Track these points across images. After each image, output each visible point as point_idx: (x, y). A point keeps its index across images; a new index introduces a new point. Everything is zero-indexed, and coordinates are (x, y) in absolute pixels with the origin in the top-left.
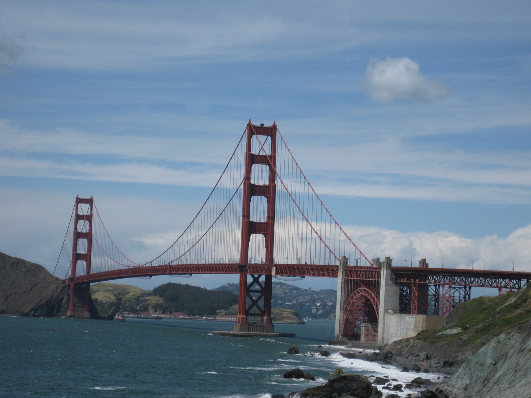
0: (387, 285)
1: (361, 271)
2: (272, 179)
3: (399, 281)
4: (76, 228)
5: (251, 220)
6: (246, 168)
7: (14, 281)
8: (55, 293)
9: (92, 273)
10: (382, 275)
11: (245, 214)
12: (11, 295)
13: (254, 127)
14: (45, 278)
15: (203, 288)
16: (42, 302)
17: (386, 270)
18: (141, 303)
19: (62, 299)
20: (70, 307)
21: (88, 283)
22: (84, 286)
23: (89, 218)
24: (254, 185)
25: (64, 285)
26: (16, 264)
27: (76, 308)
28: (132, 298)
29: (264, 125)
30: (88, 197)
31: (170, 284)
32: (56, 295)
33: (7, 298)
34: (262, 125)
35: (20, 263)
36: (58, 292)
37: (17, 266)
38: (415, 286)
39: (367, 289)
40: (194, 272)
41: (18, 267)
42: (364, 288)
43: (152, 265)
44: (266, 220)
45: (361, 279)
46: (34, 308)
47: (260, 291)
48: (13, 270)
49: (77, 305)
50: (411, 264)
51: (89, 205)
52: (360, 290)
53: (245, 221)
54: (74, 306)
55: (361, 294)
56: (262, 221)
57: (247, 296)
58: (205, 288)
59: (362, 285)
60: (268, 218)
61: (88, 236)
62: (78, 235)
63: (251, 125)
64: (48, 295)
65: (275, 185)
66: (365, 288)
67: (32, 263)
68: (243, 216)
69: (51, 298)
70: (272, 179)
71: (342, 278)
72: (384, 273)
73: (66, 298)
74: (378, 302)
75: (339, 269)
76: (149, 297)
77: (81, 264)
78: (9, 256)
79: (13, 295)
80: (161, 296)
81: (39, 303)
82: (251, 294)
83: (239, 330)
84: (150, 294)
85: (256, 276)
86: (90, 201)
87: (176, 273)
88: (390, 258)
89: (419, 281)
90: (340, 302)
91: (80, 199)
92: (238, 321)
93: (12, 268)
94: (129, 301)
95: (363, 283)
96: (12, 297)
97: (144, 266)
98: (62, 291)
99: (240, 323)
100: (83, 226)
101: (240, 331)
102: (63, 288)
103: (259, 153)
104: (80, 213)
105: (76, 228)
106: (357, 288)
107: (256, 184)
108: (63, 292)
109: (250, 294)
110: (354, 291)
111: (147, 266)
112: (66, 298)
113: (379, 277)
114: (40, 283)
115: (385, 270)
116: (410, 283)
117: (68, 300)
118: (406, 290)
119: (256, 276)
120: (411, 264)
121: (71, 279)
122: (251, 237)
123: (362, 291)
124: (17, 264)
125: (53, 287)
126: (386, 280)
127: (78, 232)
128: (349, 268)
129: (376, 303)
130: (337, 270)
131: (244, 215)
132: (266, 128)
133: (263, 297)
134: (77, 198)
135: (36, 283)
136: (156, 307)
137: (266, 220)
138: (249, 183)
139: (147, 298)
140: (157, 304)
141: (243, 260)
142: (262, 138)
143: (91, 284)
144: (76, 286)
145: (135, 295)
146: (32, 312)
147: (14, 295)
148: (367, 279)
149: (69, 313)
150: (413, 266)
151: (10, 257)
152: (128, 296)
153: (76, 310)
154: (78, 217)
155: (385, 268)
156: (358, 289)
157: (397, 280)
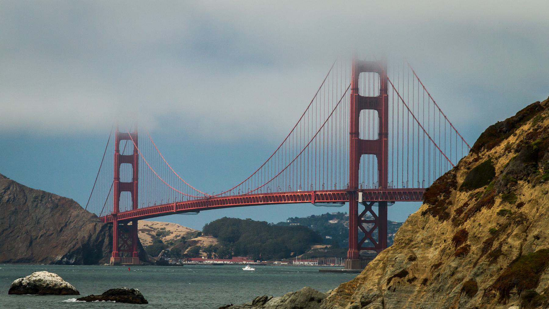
2: (384, 90)
5: (362, 137)
6: (353, 78)
7: (38, 221)
8: (93, 234)
9: (139, 207)
11: (354, 131)
12: (36, 238)
14: (78, 216)
16: (77, 247)
18: (190, 246)
19: (103, 241)
20: (114, 252)
21: (135, 221)
22: (130, 224)
25: (104, 224)
26: (40, 198)
27: (121, 253)
28: (175, 239)
31: (225, 219)
32: (94, 237)
33: (31, 242)
35: (44, 197)
36: (97, 232)
37: (41, 200)
40: (289, 202)
41: (43, 202)
44: (376, 137)
46: (67, 254)
48: (37, 206)
49: (122, 248)
53: (353, 139)
54: (119, 249)
57: (358, 227)
58: (273, 223)
60: (380, 134)
61: (133, 160)
62: (121, 159)
64: (84, 236)
65: (388, 95)
68: (351, 133)
69: (88, 240)
70: (384, 90)
73: (107, 241)
76: (199, 238)
77: (126, 196)
78: (30, 188)
79: (39, 237)
80: (215, 236)
81: (73, 248)
83: (351, 267)
84: (199, 234)
87: (264, 203)
92: (349, 257)
93: (35, 203)
94: (172, 244)
96: (38, 240)
97: (220, 196)
98: (101, 231)
101: (352, 268)
102: (103, 227)
105: (117, 150)
108: (103, 233)
111: (223, 195)
112: (107, 241)
114: (73, 222)
117: (111, 243)
119: (368, 203)
121: (115, 215)
122: (362, 158)
124: (42, 198)
125: (90, 226)
127: (120, 155)
131: (353, 133)
133: (378, 227)
135: (67, 222)
136: (210, 250)
137: (376, 137)
138: (357, 95)
139: (196, 239)
140: (211, 246)
141: (353, 185)
143: (139, 222)
144: (120, 224)
145: (179, 236)
146: (66, 259)
147: (39, 238)
149: (112, 259)
151: (31, 190)
152: (168, 238)
153: (121, 255)
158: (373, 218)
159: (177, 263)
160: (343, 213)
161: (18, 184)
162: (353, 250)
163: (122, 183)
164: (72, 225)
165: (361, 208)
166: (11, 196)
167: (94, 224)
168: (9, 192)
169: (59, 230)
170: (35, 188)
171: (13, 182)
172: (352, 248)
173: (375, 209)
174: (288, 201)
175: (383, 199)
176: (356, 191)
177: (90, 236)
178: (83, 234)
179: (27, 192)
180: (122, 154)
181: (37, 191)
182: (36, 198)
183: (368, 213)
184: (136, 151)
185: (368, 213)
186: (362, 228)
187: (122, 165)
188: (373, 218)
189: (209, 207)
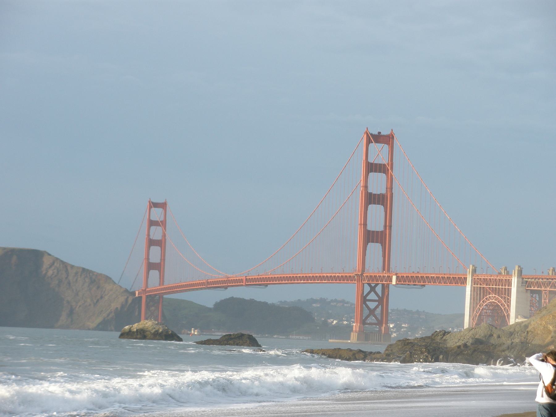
0: (518, 292)
1: (490, 279)
2: (390, 188)
3: (529, 288)
4: (149, 235)
10: (513, 283)
11: (362, 223)
13: (371, 134)
15: (270, 304)
16: (110, 316)
17: (517, 278)
23: (163, 224)
24: (371, 194)
29: (382, 134)
30: (162, 201)
31: (232, 299)
34: (379, 133)
36: (128, 304)
37: (81, 275)
38: (545, 293)
39: (497, 296)
40: (301, 282)
42: (494, 295)
43: (248, 274)
45: (491, 286)
47: (368, 301)
48: (77, 280)
50: (543, 272)
51: (162, 209)
52: (489, 297)
55: (491, 301)
56: (377, 230)
59: (492, 293)
60: (385, 226)
61: (160, 243)
62: (151, 243)
63: (369, 134)
66: (495, 296)
67: (98, 273)
71: (471, 285)
72: (515, 281)
74: (509, 309)
75: (468, 277)
77: (154, 274)
79: (78, 307)
82: (367, 303)
84: (209, 310)
85: (373, 285)
86: (163, 206)
88: (521, 267)
89: (549, 288)
90: (469, 309)
91: (152, 203)
92: (355, 331)
95: (493, 291)
99: (357, 332)
100: (156, 233)
103: (374, 161)
104: (152, 218)
105: (149, 235)
106: (486, 296)
107: (374, 192)
109: (367, 303)
110: (484, 298)
113: (510, 284)
115: (516, 278)
116: (540, 291)
118: (536, 297)
119: (373, 285)
120: (543, 272)
121: (144, 291)
123: (491, 298)
125: (122, 299)
126: (518, 287)
127: (150, 239)
128: (478, 276)
129: (507, 309)
130: (465, 279)
132: (384, 136)
134: (149, 202)
142: (380, 146)
148: (497, 287)
150: (543, 275)
151: (72, 267)
154: (152, 223)
155: (516, 276)
156: (488, 296)
157: (528, 287)
158: (377, 298)
159: (196, 333)
160: (324, 299)
161: (62, 261)
162: (359, 324)
163: (151, 263)
164: (106, 298)
165: (367, 289)
166: (55, 271)
167: (126, 297)
168: (53, 268)
169: (95, 301)
170: (76, 264)
171: (57, 259)
172: (358, 323)
173: (379, 289)
174: (300, 281)
175: (387, 282)
176: (363, 274)
177: (123, 306)
178: (116, 305)
179: (69, 268)
180: (152, 238)
181: (78, 268)
182: (76, 273)
183: (373, 293)
184: (164, 235)
185: (373, 293)
186: (367, 307)
187: (152, 248)
188: (377, 298)
189: (228, 285)
